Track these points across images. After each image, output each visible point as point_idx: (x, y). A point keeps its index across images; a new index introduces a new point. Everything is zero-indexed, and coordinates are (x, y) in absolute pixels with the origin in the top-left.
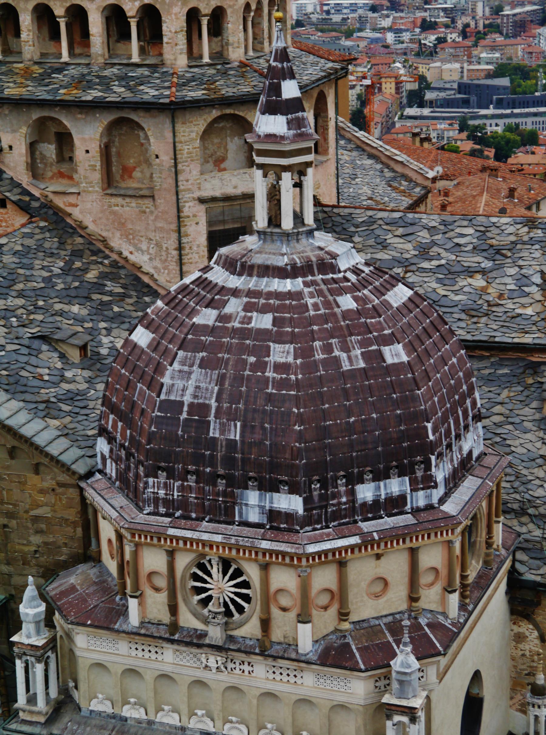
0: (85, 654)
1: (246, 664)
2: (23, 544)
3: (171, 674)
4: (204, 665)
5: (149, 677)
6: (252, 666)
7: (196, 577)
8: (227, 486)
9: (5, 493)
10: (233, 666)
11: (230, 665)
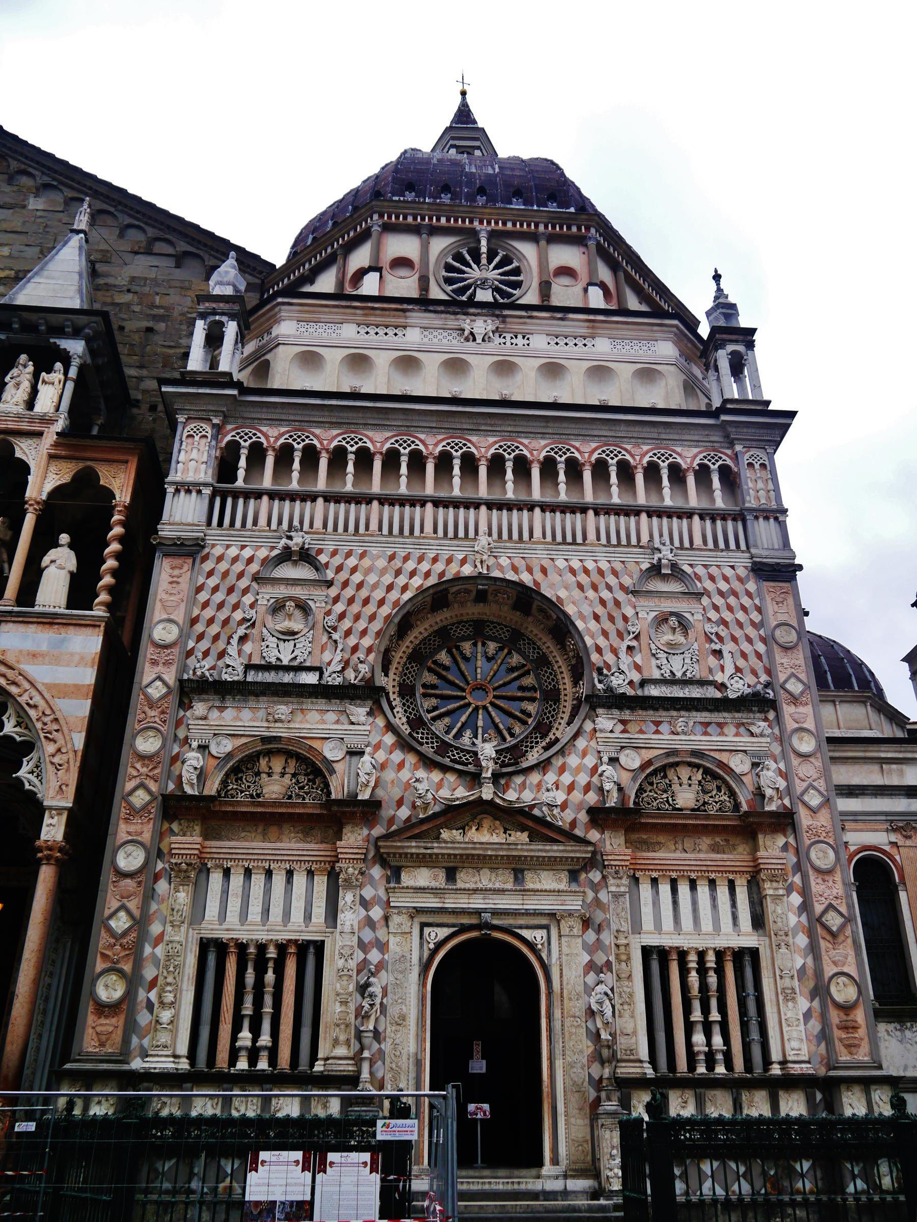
0: (292, 340)
1: (520, 336)
2: (170, 347)
4: (466, 333)
5: (382, 360)
6: (528, 339)
7: (449, 268)
10: (504, 341)
11: (497, 340)
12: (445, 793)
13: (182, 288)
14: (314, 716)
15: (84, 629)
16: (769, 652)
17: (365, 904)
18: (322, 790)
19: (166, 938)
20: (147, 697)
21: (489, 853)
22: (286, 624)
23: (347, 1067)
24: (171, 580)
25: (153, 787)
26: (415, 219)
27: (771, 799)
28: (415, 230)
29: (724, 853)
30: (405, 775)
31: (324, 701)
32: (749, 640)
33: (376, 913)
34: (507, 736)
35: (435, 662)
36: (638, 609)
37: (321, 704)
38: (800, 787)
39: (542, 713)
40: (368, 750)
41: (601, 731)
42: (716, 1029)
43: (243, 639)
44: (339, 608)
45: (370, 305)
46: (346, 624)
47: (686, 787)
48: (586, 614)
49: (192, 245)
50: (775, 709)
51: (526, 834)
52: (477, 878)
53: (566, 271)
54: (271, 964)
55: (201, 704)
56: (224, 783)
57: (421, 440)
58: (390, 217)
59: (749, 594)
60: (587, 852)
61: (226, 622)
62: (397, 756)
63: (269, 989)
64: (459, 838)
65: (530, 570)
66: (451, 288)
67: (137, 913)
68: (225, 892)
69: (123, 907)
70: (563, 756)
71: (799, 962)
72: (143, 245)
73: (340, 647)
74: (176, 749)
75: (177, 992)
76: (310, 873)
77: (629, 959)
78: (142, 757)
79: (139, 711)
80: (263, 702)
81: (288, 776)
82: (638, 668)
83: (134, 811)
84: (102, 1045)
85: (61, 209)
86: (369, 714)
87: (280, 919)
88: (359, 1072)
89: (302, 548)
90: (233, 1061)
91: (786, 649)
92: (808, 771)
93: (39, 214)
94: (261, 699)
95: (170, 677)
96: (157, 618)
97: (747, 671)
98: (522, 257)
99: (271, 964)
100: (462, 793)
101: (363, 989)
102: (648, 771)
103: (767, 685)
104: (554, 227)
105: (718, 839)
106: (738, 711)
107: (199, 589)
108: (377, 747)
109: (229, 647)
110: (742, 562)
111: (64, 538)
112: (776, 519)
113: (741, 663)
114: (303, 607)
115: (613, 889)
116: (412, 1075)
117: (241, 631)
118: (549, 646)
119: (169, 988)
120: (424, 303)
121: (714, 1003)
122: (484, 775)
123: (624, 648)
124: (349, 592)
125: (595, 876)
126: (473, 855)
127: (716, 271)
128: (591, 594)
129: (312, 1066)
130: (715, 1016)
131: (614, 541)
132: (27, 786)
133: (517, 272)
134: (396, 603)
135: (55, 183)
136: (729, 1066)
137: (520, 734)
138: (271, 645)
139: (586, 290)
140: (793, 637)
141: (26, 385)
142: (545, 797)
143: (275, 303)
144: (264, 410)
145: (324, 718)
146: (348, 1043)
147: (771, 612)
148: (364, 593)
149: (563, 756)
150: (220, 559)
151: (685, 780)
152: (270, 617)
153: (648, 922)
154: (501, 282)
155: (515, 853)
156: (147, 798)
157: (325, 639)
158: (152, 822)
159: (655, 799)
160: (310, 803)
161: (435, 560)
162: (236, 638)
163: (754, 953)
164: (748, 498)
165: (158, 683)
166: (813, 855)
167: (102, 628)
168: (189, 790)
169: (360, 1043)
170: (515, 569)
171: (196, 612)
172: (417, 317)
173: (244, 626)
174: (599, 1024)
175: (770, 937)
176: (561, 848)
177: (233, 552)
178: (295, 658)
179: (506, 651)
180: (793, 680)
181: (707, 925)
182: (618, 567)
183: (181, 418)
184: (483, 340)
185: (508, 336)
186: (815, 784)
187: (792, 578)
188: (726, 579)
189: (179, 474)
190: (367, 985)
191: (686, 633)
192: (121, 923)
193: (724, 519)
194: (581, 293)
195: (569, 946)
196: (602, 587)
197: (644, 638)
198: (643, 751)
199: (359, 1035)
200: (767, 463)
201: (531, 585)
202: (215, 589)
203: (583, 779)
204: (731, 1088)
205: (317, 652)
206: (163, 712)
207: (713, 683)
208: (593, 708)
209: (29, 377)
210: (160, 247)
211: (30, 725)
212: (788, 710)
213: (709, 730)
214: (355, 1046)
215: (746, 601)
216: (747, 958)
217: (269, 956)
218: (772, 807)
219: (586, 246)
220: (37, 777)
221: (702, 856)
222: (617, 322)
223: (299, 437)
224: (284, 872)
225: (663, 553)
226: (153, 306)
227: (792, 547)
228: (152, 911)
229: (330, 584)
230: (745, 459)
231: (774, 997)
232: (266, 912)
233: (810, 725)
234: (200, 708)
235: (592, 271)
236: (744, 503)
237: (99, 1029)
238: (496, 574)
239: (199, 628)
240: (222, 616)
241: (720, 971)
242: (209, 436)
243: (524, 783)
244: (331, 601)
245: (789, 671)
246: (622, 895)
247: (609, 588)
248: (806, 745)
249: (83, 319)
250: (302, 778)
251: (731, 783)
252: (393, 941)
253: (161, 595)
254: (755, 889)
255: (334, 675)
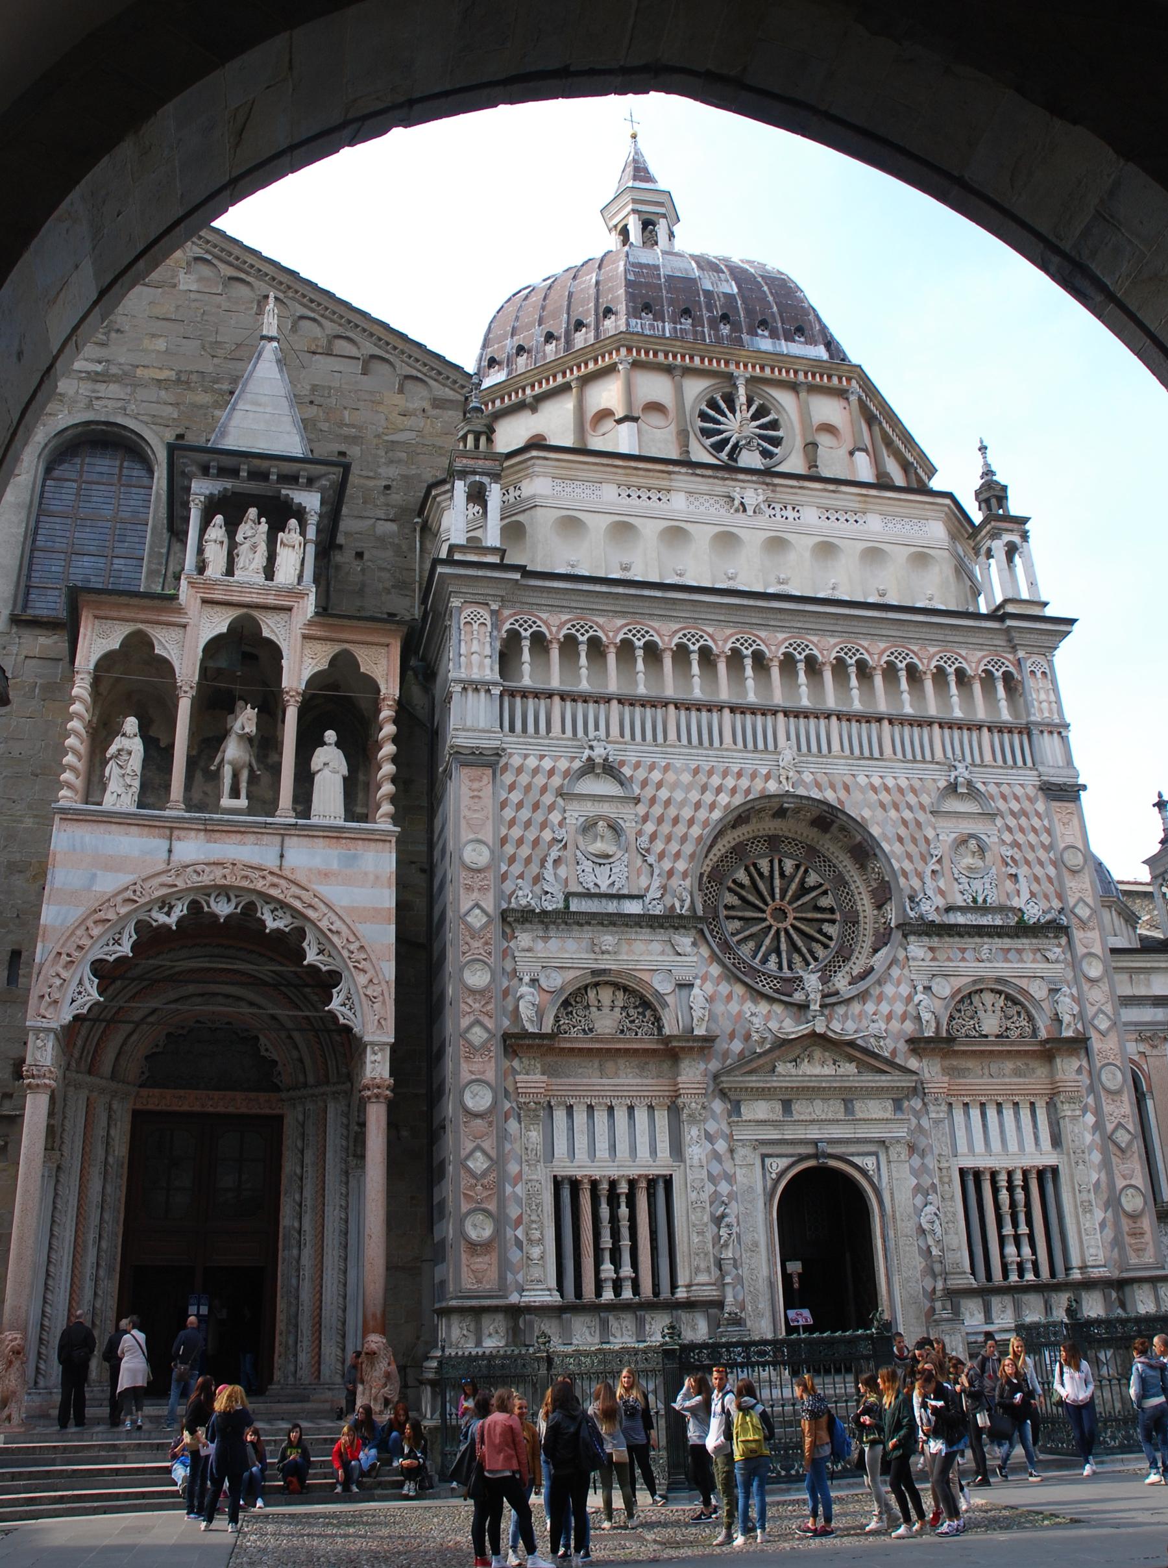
0: (550, 502)
1: (789, 508)
2: (368, 477)
3: (682, 525)
4: (737, 503)
5: (650, 530)
7: (703, 416)
8: (732, 331)
9: (346, 413)
10: (773, 512)
12: (773, 1025)
13: (373, 402)
14: (639, 946)
15: (373, 844)
16: (1059, 875)
17: (709, 1138)
18: (653, 1024)
19: (524, 1177)
20: (468, 926)
21: (824, 1085)
22: (599, 846)
23: (711, 1293)
24: (472, 794)
25: (490, 1024)
26: (666, 356)
27: (1069, 1025)
28: (668, 370)
29: (1025, 1077)
30: (734, 1007)
31: (648, 930)
32: (1041, 864)
33: (721, 1146)
34: (811, 961)
35: (734, 881)
36: (939, 831)
37: (645, 934)
38: (1091, 1011)
39: (842, 935)
40: (698, 982)
41: (914, 959)
42: (1025, 1241)
43: (557, 862)
44: (650, 827)
45: (633, 464)
46: (659, 846)
47: (990, 1013)
48: (890, 835)
49: (380, 347)
50: (1067, 935)
51: (854, 1065)
52: (811, 1109)
53: (829, 429)
54: (623, 1199)
55: (524, 935)
56: (557, 1019)
57: (709, 635)
58: (638, 352)
59: (1038, 815)
60: (911, 1081)
61: (536, 842)
62: (724, 988)
63: (624, 1224)
64: (793, 1071)
65: (833, 787)
66: (709, 442)
67: (493, 1154)
68: (571, 1129)
69: (478, 1148)
70: (880, 985)
71: (1094, 1177)
72: (324, 342)
73: (657, 872)
74: (505, 984)
75: (541, 1229)
76: (651, 1108)
77: (951, 1180)
78: (472, 992)
79: (461, 942)
80: (587, 933)
81: (618, 1010)
82: (942, 893)
83: (473, 1050)
84: (479, 1281)
85: (219, 291)
86: (694, 944)
87: (627, 1155)
88: (725, 1297)
89: (606, 760)
90: (599, 1294)
91: (1074, 872)
92: (1097, 995)
93: (193, 295)
94: (586, 928)
95: (489, 904)
96: (464, 839)
97: (1040, 896)
98: (781, 409)
99: (623, 1199)
100: (792, 1028)
101: (718, 1220)
102: (958, 998)
103: (1061, 911)
104: (814, 376)
105: (1019, 1064)
106: (1036, 937)
107: (504, 805)
108: (704, 979)
109: (545, 872)
110: (1030, 780)
111: (330, 736)
112: (1059, 733)
113: (1035, 887)
114: (615, 829)
115: (933, 1115)
116: (768, 1296)
117: (554, 854)
118: (847, 865)
119: (534, 1226)
120: (687, 463)
121: (1022, 1218)
122: (812, 1007)
123: (929, 873)
124: (657, 810)
125: (917, 1103)
126: (808, 1088)
127: (981, 442)
128: (893, 813)
129: (673, 1293)
130: (1023, 1229)
131: (909, 756)
132: (342, 1021)
133: (774, 425)
134: (706, 823)
135: (209, 257)
136: (1037, 1274)
137: (824, 959)
138: (587, 870)
139: (851, 453)
140: (1080, 860)
141: (262, 548)
142: (874, 1028)
143: (528, 455)
144: (545, 595)
145: (650, 948)
146: (708, 1270)
147: (1059, 834)
148: (672, 812)
149: (880, 985)
150: (520, 770)
151: (990, 1008)
152: (580, 839)
153: (962, 1147)
154: (761, 437)
155: (847, 1084)
156: (485, 1035)
157: (639, 862)
158: (493, 1060)
159: (964, 1026)
160: (645, 1039)
161: (739, 775)
162: (550, 860)
163: (1055, 1170)
164: (1033, 711)
165: (477, 911)
166: (1104, 1078)
167: (393, 844)
168: (531, 1029)
169: (721, 1270)
170: (818, 785)
171: (504, 831)
172: (683, 479)
173: (555, 848)
174: (931, 1242)
175: (1068, 1154)
176: (889, 1078)
177: (532, 762)
178: (613, 884)
179: (802, 869)
180: (1081, 904)
181: (1013, 1146)
182: (917, 784)
183: (455, 602)
184: (755, 512)
185: (778, 506)
186: (1103, 1008)
187: (1076, 799)
188: (1017, 798)
189: (463, 670)
190: (723, 1216)
191: (983, 858)
192: (478, 1164)
193: (1010, 732)
194: (847, 456)
195: (898, 1171)
196: (902, 806)
197: (946, 861)
198: (952, 978)
199: (719, 1264)
200: (1047, 671)
201: (835, 803)
202: (520, 805)
203: (899, 1008)
204: (1042, 1292)
205: (633, 876)
206: (486, 943)
207: (1012, 909)
208: (905, 936)
209: (264, 537)
210: (342, 346)
211: (334, 953)
212: (1078, 934)
213: (1009, 956)
214: (715, 1272)
215: (1036, 822)
216: (1049, 1175)
217: (619, 1191)
218: (1068, 1033)
219: (847, 399)
220: (351, 1009)
221: (1007, 1080)
222: (889, 498)
223: (582, 627)
224: (625, 1108)
225: (960, 770)
226: (342, 424)
227: (1076, 764)
228: (506, 1151)
229: (637, 800)
230: (1028, 665)
231: (1072, 1210)
232: (613, 1148)
233: (1097, 949)
234: (524, 938)
235: (856, 434)
236: (1028, 714)
237: (474, 1267)
238: (801, 791)
239: (509, 849)
240: (531, 835)
241: (1026, 1188)
242: (489, 623)
243: (846, 1015)
244: (640, 821)
245: (1078, 895)
246: (941, 1121)
247: (910, 807)
248: (1094, 970)
249: (322, 469)
250: (632, 1012)
251: (1031, 1008)
252: (738, 1171)
253: (464, 812)
254: (1052, 1110)
255: (654, 902)
